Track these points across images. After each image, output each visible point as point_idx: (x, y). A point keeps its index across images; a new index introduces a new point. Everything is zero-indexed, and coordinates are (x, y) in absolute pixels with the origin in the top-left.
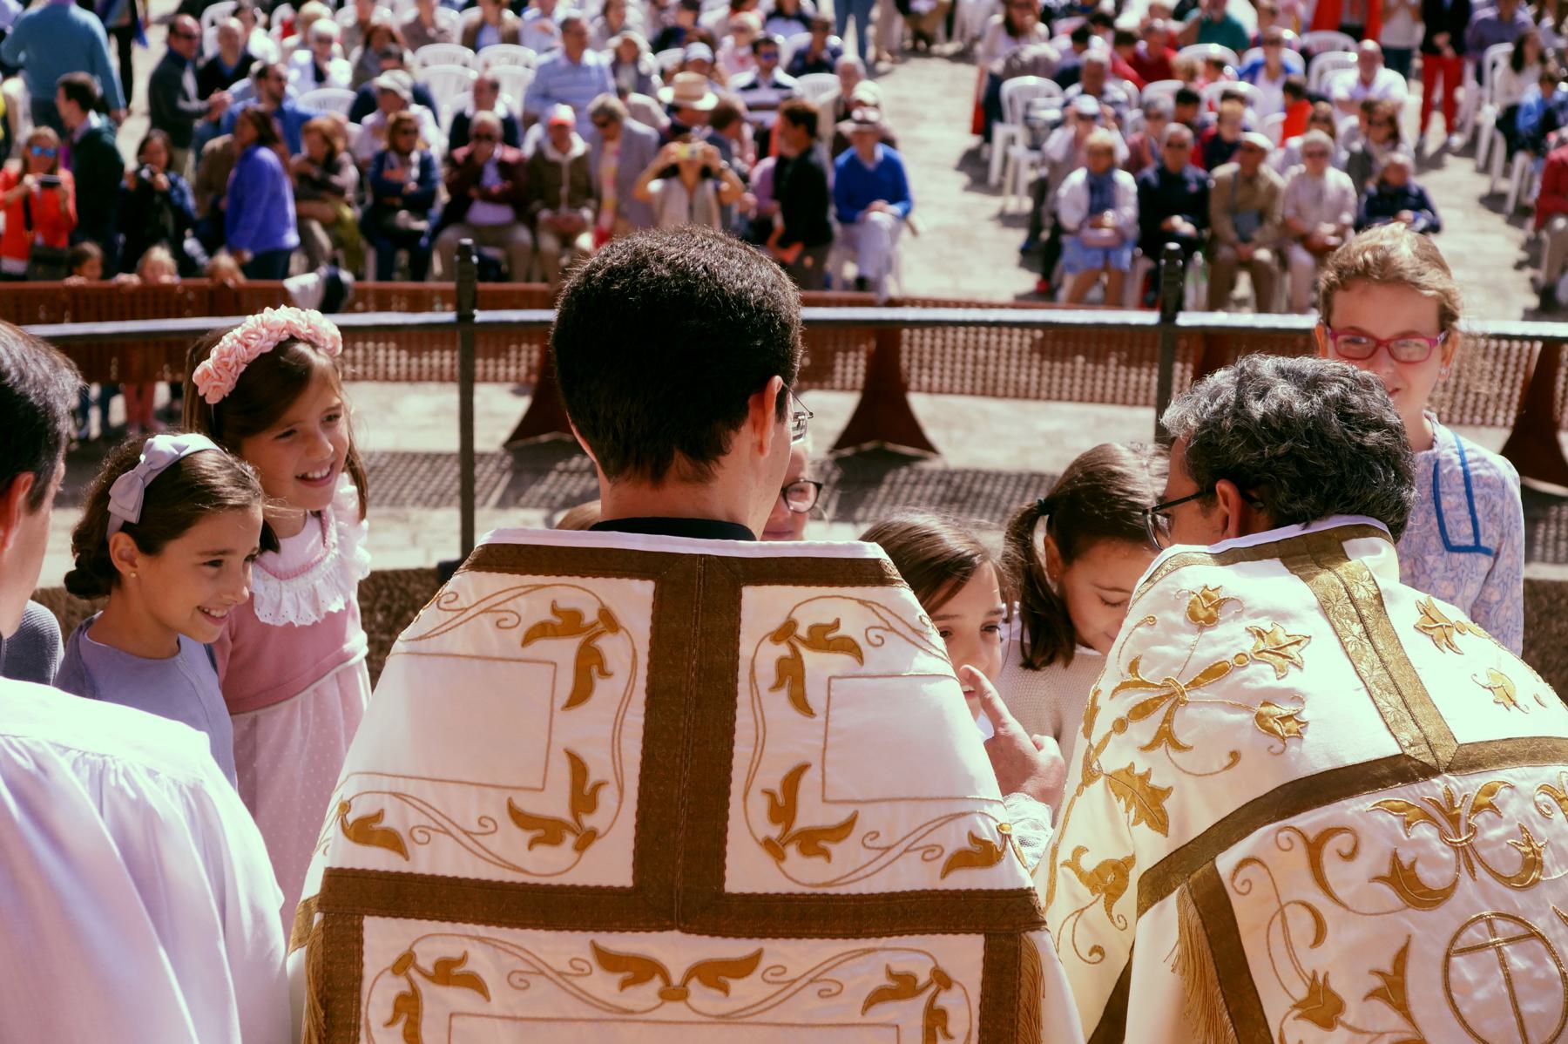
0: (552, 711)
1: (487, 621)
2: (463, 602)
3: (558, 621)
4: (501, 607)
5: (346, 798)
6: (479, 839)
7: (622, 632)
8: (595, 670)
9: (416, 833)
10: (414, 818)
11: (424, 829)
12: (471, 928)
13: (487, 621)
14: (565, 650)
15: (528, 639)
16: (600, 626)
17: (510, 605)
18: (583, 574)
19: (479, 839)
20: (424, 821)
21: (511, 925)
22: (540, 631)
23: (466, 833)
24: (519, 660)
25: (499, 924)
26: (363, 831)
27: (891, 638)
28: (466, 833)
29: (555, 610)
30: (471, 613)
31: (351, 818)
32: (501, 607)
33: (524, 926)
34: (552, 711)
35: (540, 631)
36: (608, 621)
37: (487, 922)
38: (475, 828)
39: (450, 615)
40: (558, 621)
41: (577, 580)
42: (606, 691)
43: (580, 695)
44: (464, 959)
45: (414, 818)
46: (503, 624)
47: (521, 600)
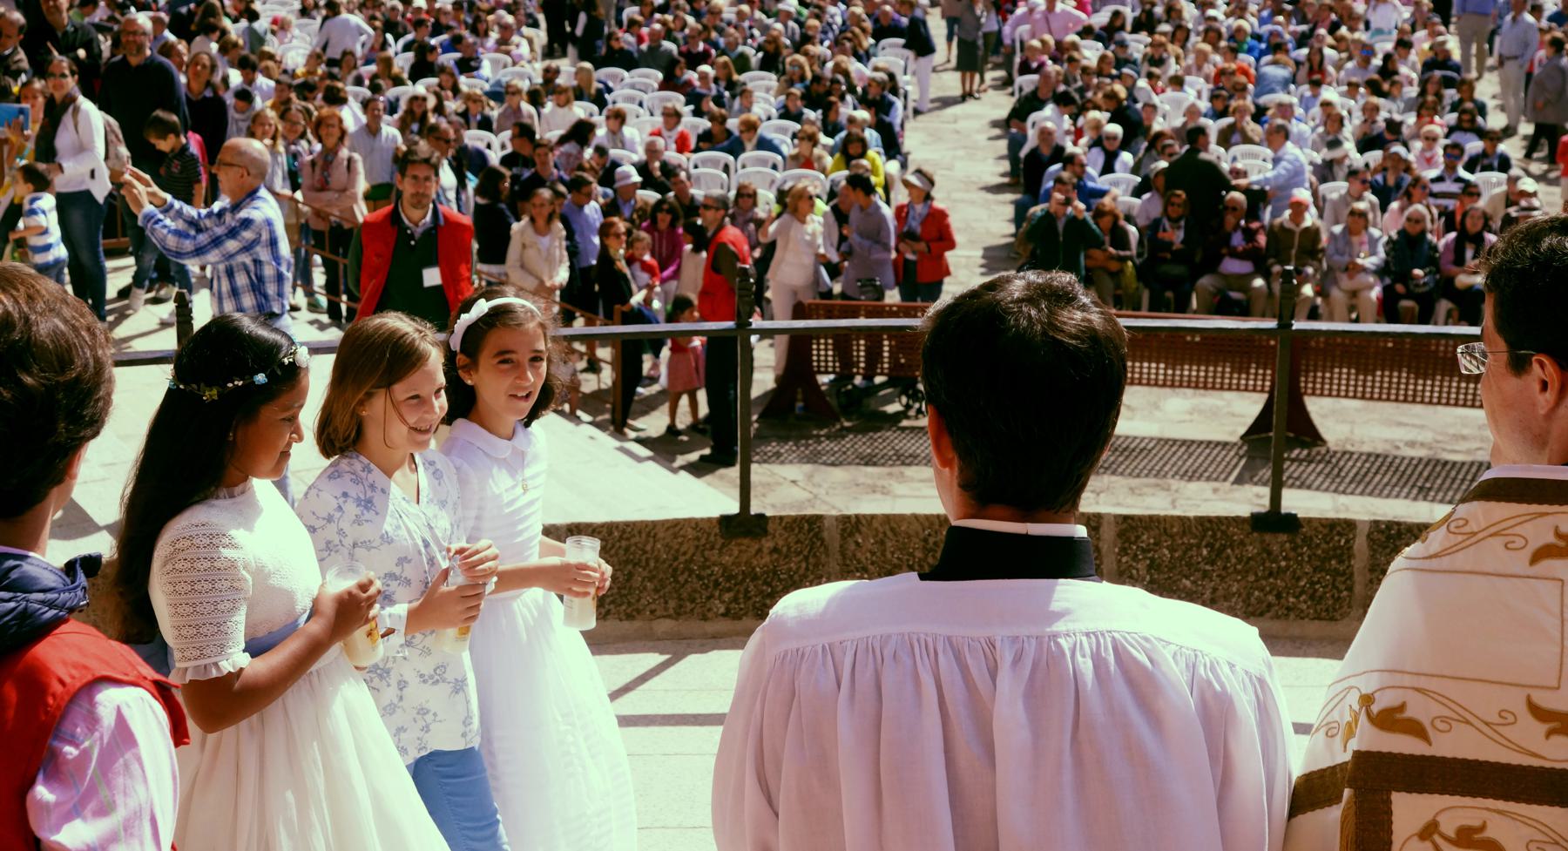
5: (1366, 690)
6: (1500, 729)
9: (1438, 723)
10: (1438, 710)
11: (1444, 719)
12: (1490, 803)
19: (1500, 729)
20: (1447, 713)
21: (1528, 802)
23: (1487, 724)
25: (1517, 800)
26: (1389, 720)
28: (1487, 724)
31: (1375, 709)
33: (1540, 803)
37: (1506, 798)
38: (1496, 719)
44: (1483, 828)
45: (1438, 710)
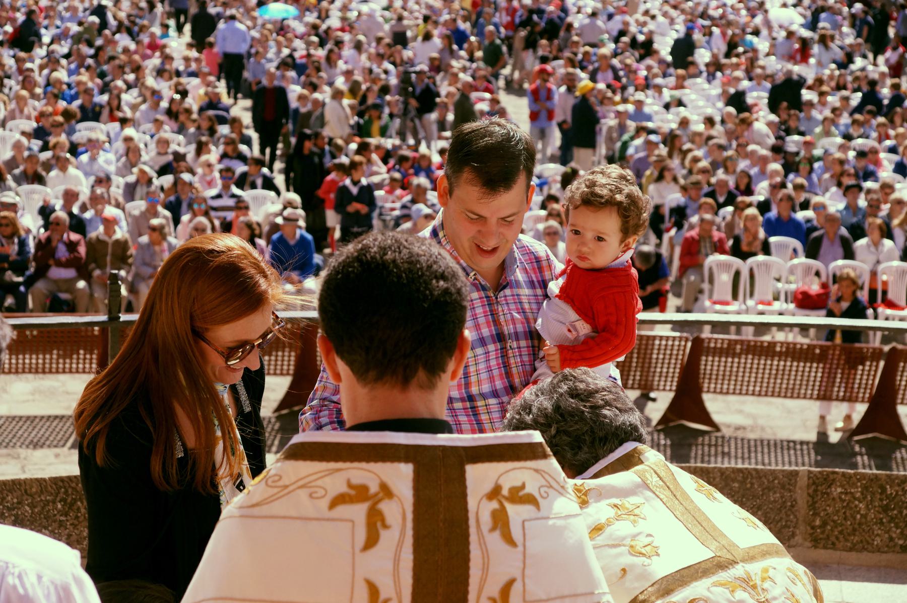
0: (354, 554)
1: (303, 494)
2: (285, 481)
3: (353, 492)
4: (313, 484)
7: (395, 498)
8: (379, 524)
13: (303, 494)
14: (358, 512)
15: (334, 504)
16: (381, 495)
17: (319, 483)
18: (368, 460)
22: (339, 500)
24: (328, 520)
27: (551, 491)
29: (350, 485)
30: (291, 488)
32: (313, 484)
34: (354, 554)
35: (339, 500)
36: (386, 491)
39: (276, 490)
40: (353, 492)
41: (364, 465)
42: (388, 539)
43: (372, 541)
46: (315, 495)
47: (327, 480)
